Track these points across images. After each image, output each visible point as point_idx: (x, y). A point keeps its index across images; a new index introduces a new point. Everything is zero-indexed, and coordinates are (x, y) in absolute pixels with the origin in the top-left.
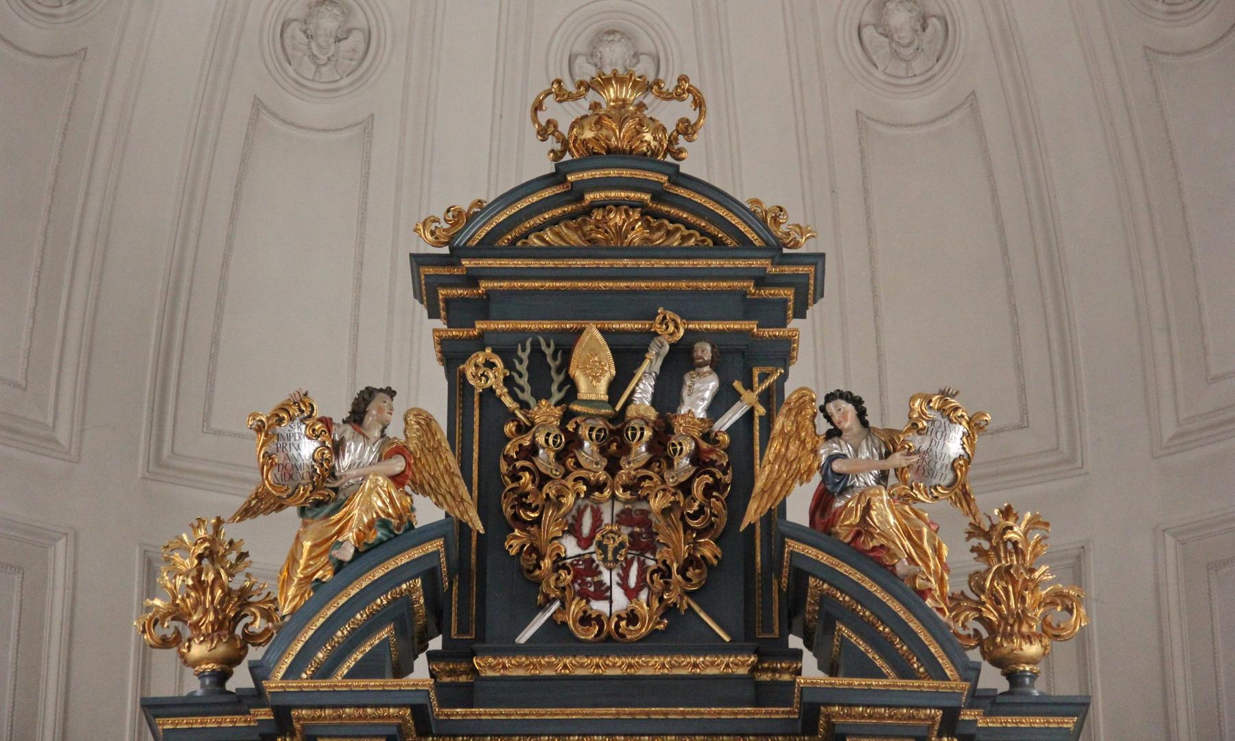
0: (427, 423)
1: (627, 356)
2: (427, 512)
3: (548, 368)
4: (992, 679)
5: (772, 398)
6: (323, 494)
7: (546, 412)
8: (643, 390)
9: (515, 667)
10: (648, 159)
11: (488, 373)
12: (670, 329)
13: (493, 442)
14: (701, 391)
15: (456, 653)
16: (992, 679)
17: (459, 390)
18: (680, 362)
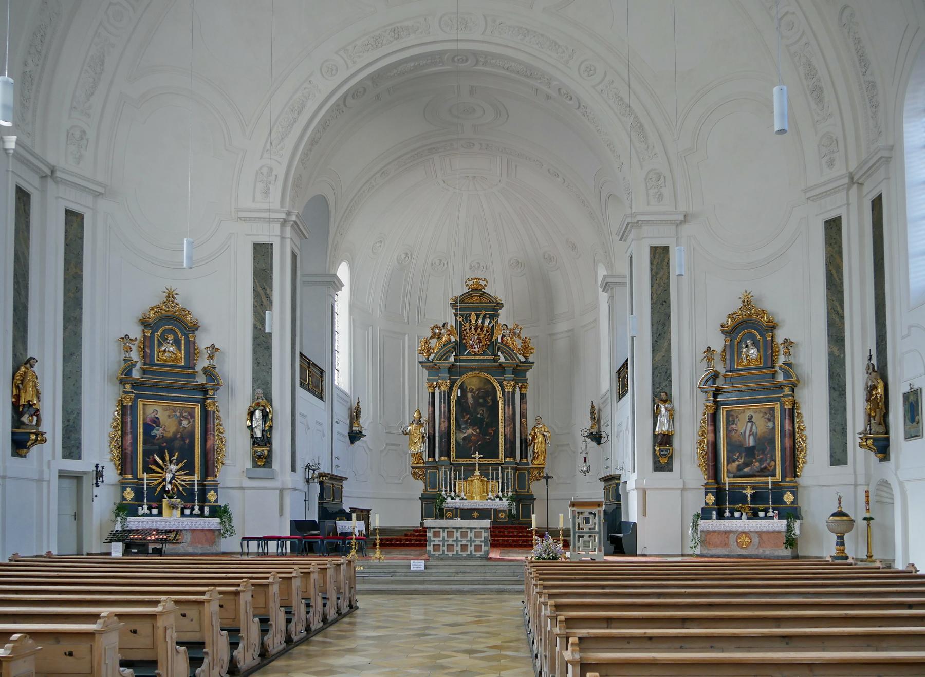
0: (451, 326)
1: (478, 316)
2: (453, 339)
3: (467, 318)
4: (523, 359)
5: (496, 322)
6: (439, 337)
7: (467, 324)
8: (480, 321)
9: (465, 358)
10: (480, 290)
11: (460, 319)
12: (483, 313)
13: (461, 328)
14: (487, 321)
15: (456, 356)
16: (523, 359)
17: (456, 321)
18: (484, 317)
